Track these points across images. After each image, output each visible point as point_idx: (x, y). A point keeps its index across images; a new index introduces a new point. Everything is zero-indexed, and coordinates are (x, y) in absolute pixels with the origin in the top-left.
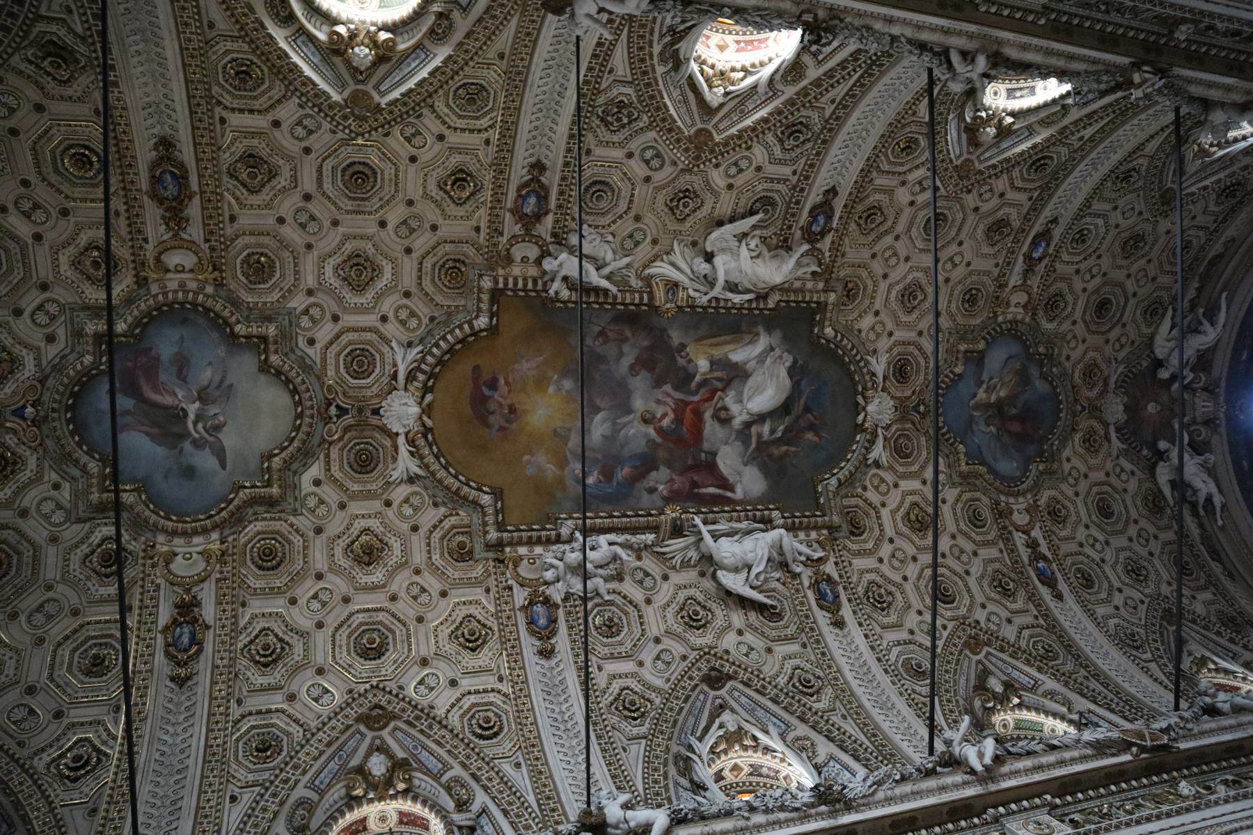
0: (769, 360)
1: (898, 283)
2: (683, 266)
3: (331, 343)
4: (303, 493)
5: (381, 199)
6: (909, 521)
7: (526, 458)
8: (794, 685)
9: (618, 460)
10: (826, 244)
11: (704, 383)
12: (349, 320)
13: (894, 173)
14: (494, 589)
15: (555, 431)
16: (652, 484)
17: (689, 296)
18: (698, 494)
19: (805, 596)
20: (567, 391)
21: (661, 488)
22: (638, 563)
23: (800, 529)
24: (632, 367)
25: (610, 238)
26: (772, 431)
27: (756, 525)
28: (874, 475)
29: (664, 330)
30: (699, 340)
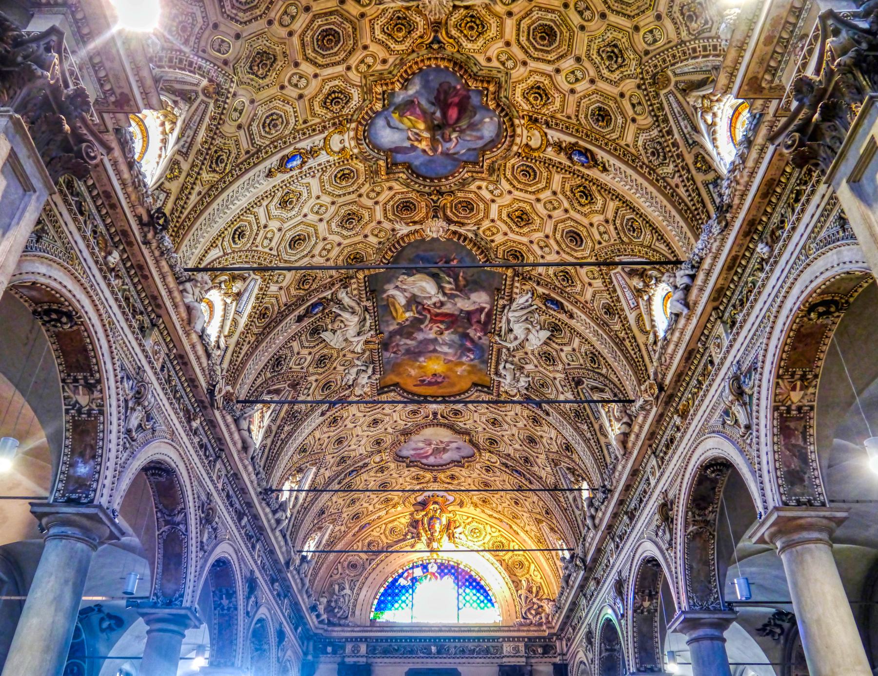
0: (404, 287)
11: (419, 313)
24: (412, 340)
26: (450, 283)
28: (484, 233)
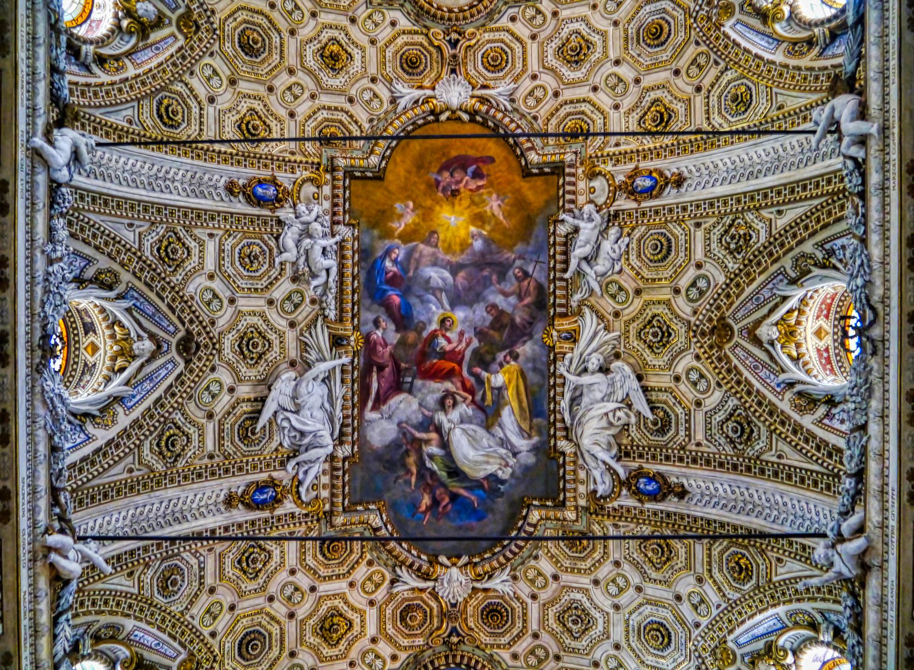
0: (503, 451)
1: (590, 599)
2: (594, 344)
3: (512, 34)
4: (385, 11)
5: (639, 55)
6: (332, 616)
7: (411, 204)
8: (170, 428)
9: (406, 292)
10: (627, 501)
11: (480, 381)
12: (533, 49)
13: (709, 563)
14: (293, 158)
15: (435, 232)
16: (383, 324)
17: (565, 354)
18: (371, 371)
19: (261, 471)
20: (471, 245)
21: (379, 333)
22: (308, 300)
23: (333, 477)
24: (494, 306)
25: (617, 268)
26: (431, 457)
27: (338, 427)
28: (383, 576)
29: (531, 336)
30: (522, 374)
